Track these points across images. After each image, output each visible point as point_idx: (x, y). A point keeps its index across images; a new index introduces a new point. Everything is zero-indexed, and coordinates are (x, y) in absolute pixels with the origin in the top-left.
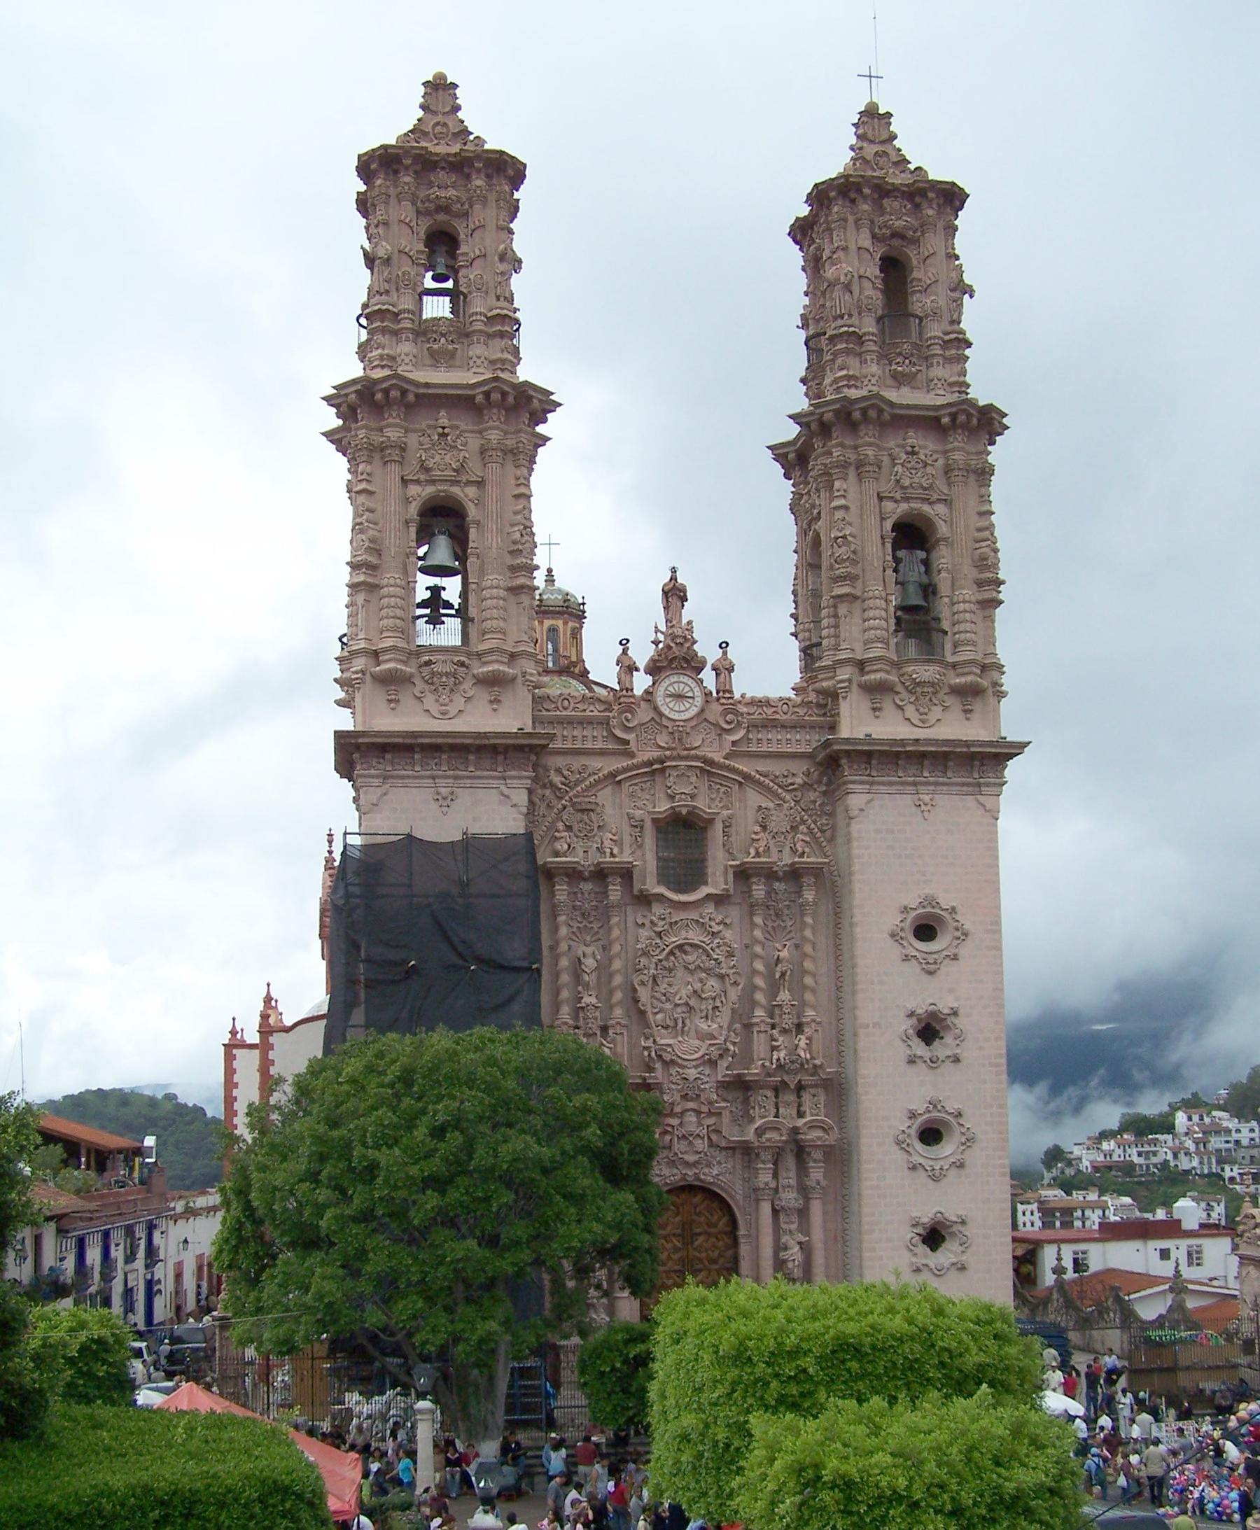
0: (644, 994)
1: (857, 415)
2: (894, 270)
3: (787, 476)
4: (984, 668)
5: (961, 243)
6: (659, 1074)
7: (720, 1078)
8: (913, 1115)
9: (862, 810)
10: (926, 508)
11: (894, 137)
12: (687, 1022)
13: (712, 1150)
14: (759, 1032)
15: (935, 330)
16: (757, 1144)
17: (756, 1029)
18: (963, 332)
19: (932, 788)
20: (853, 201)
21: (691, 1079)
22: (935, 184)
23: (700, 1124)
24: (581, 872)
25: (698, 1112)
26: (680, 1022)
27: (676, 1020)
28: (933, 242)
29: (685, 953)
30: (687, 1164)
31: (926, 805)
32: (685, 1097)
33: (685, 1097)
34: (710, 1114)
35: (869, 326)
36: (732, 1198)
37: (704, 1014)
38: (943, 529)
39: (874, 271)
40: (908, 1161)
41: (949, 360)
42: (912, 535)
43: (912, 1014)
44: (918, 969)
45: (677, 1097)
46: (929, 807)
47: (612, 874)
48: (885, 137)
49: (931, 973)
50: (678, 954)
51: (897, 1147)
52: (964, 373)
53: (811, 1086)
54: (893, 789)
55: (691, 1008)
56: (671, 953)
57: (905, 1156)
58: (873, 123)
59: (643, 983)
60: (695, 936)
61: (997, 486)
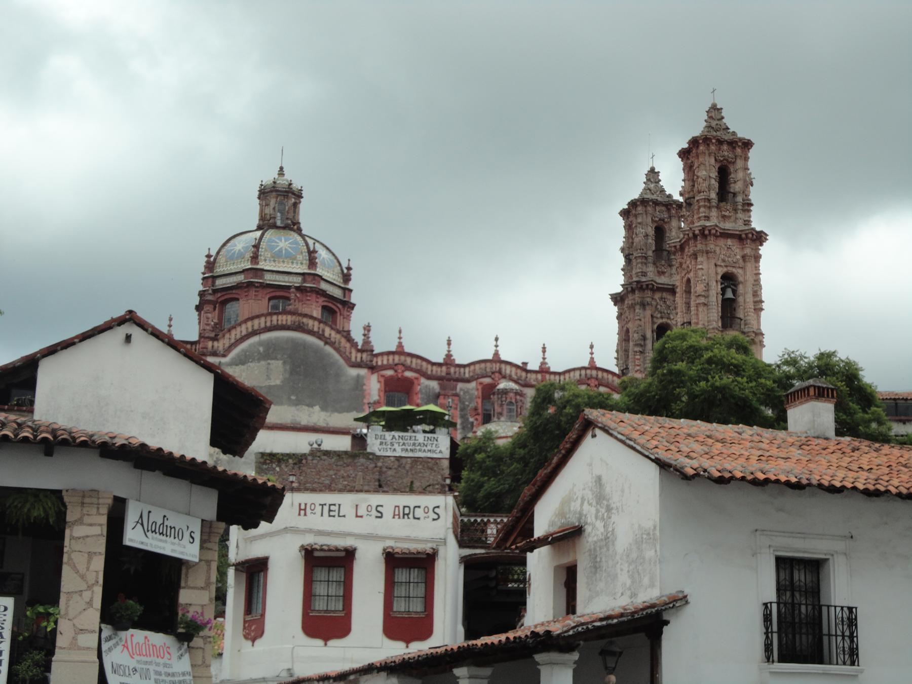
1: (707, 232)
2: (724, 174)
3: (615, 305)
4: (756, 334)
5: (750, 164)
10: (734, 270)
11: (723, 118)
15: (739, 199)
18: (750, 200)
20: (708, 145)
22: (740, 139)
28: (740, 163)
35: (713, 195)
38: (741, 279)
39: (714, 174)
41: (744, 211)
42: (729, 280)
48: (719, 117)
52: (750, 217)
58: (715, 112)
61: (762, 263)
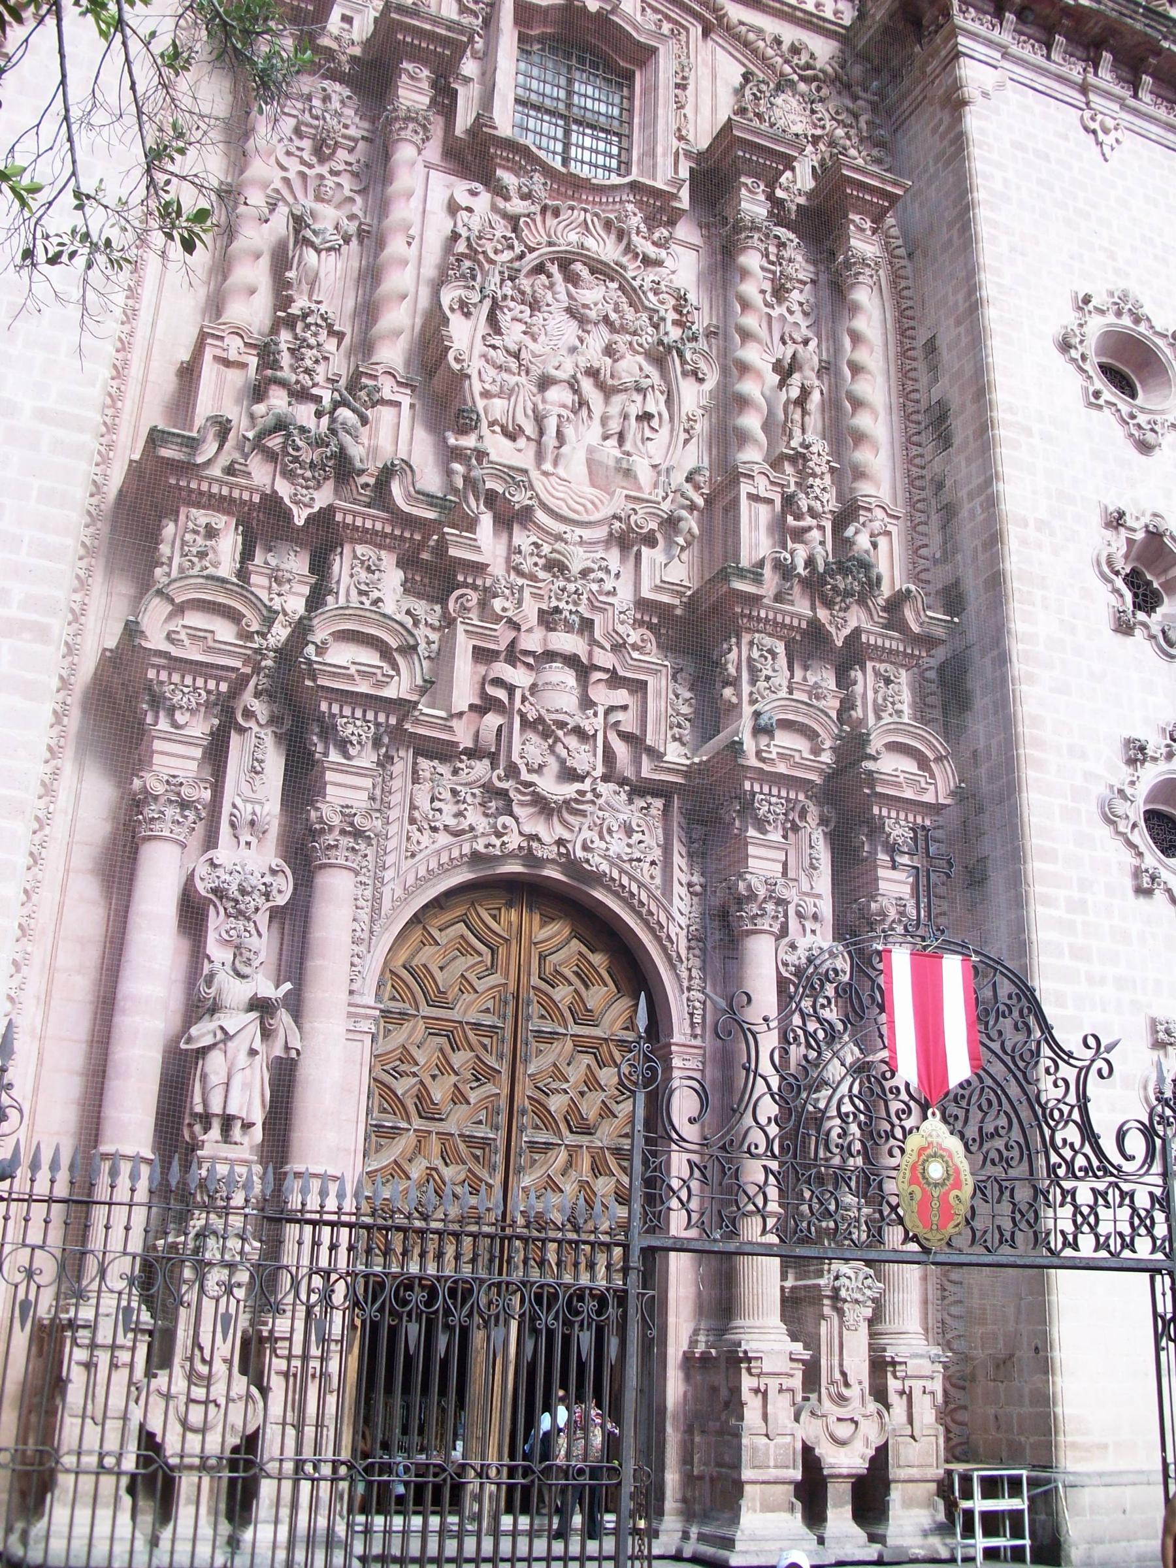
0: (463, 334)
6: (486, 543)
7: (646, 593)
8: (1136, 754)
9: (985, 95)
12: (569, 431)
13: (612, 786)
14: (754, 498)
16: (753, 762)
17: (745, 488)
19: (1116, 107)
21: (575, 567)
23: (587, 703)
24: (329, 54)
25: (582, 669)
26: (551, 424)
27: (539, 420)
29: (572, 279)
30: (544, 806)
31: (1106, 131)
32: (549, 619)
33: (549, 619)
34: (615, 680)
36: (655, 930)
37: (614, 426)
40: (1137, 873)
43: (1116, 521)
44: (1119, 432)
45: (530, 610)
46: (1108, 139)
47: (418, 56)
49: (1145, 447)
50: (558, 277)
51: (1107, 830)
53: (887, 655)
54: (1042, 82)
55: (583, 403)
56: (539, 269)
57: (1128, 859)
59: (465, 308)
60: (607, 250)
